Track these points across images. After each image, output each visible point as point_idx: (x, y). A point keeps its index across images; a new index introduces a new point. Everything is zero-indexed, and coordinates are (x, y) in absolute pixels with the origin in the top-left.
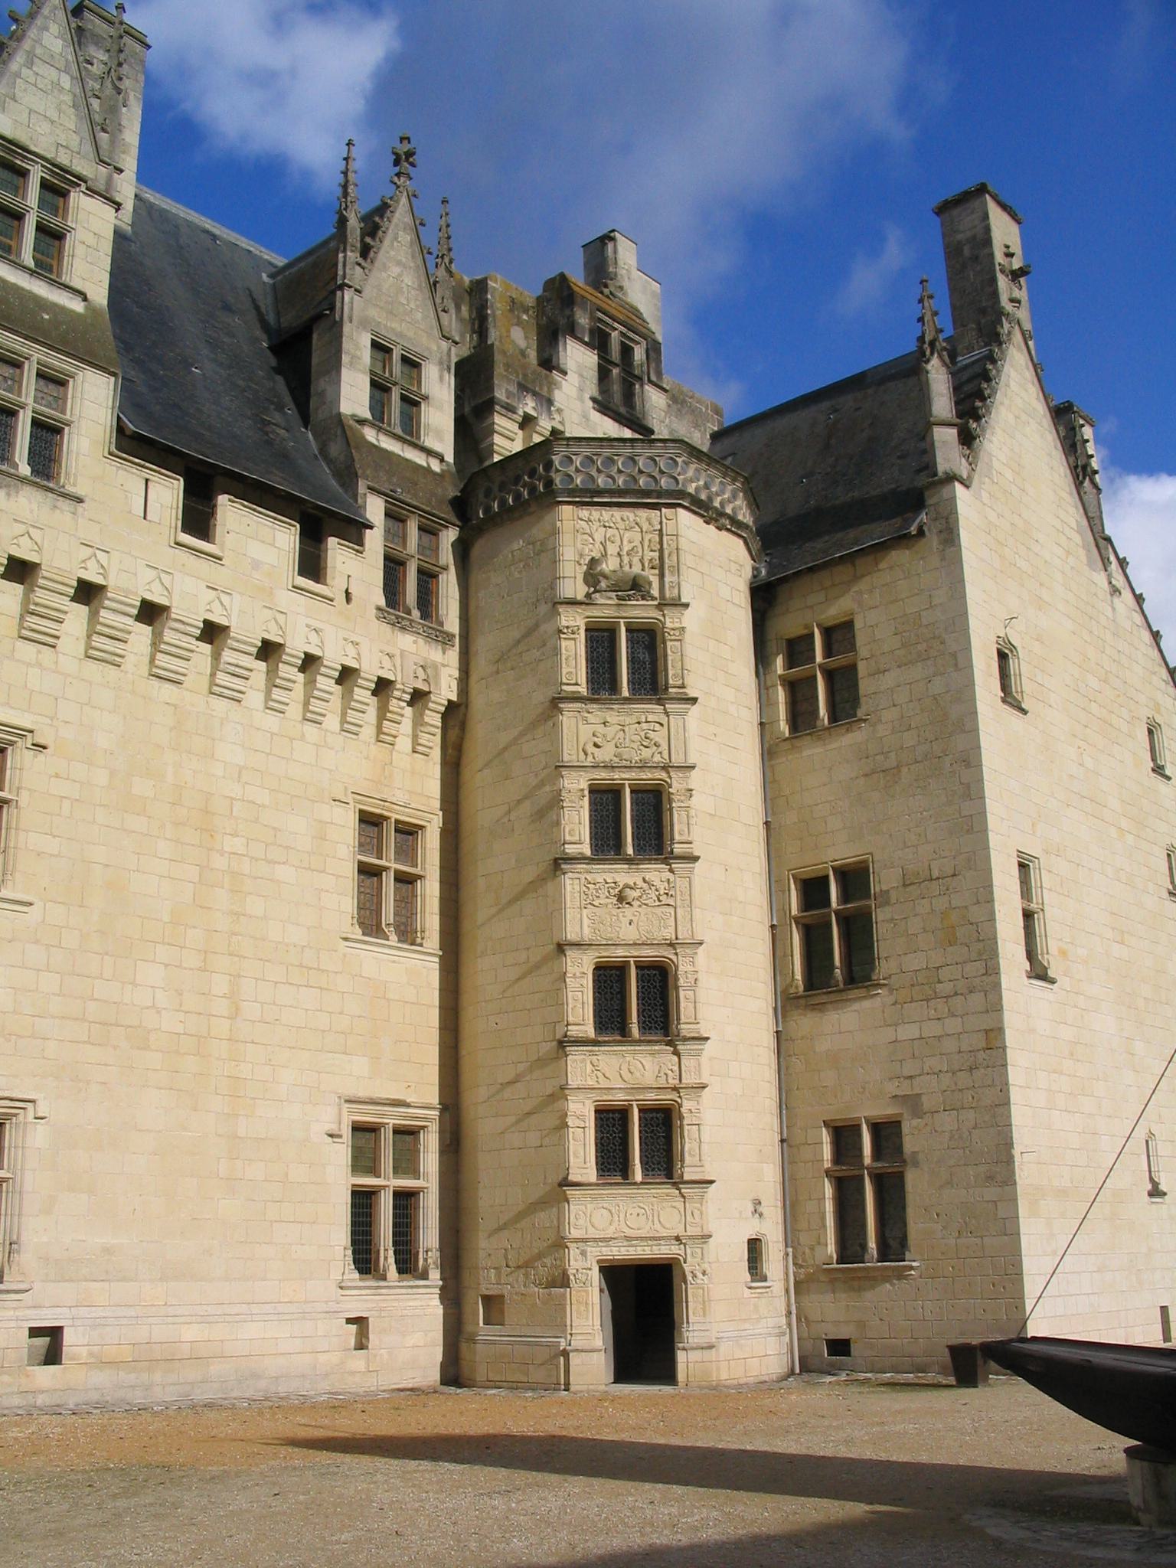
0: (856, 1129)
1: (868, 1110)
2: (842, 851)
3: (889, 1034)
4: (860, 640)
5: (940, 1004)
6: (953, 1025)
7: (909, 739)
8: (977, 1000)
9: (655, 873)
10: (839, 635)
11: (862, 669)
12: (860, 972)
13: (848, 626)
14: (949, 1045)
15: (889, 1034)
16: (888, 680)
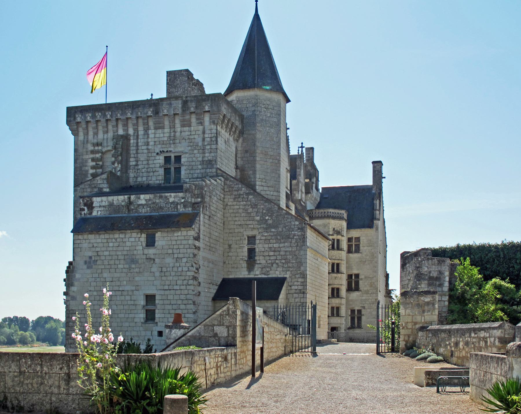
0: (354, 310)
1: (356, 308)
2: (355, 272)
3: (361, 298)
4: (361, 241)
5: (369, 295)
6: (370, 298)
7: (368, 257)
8: (374, 295)
9: (339, 275)
10: (358, 239)
11: (361, 245)
12: (357, 289)
13: (359, 238)
14: (370, 300)
15: (361, 298)
16: (365, 248)
